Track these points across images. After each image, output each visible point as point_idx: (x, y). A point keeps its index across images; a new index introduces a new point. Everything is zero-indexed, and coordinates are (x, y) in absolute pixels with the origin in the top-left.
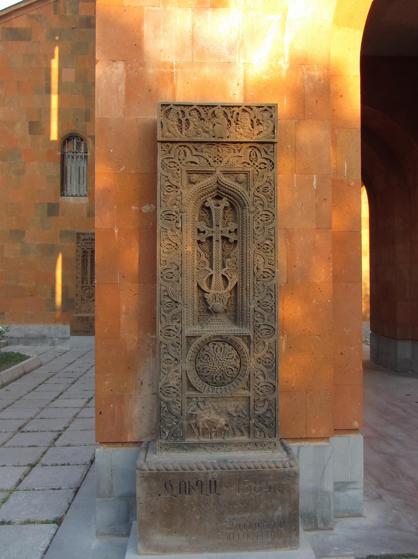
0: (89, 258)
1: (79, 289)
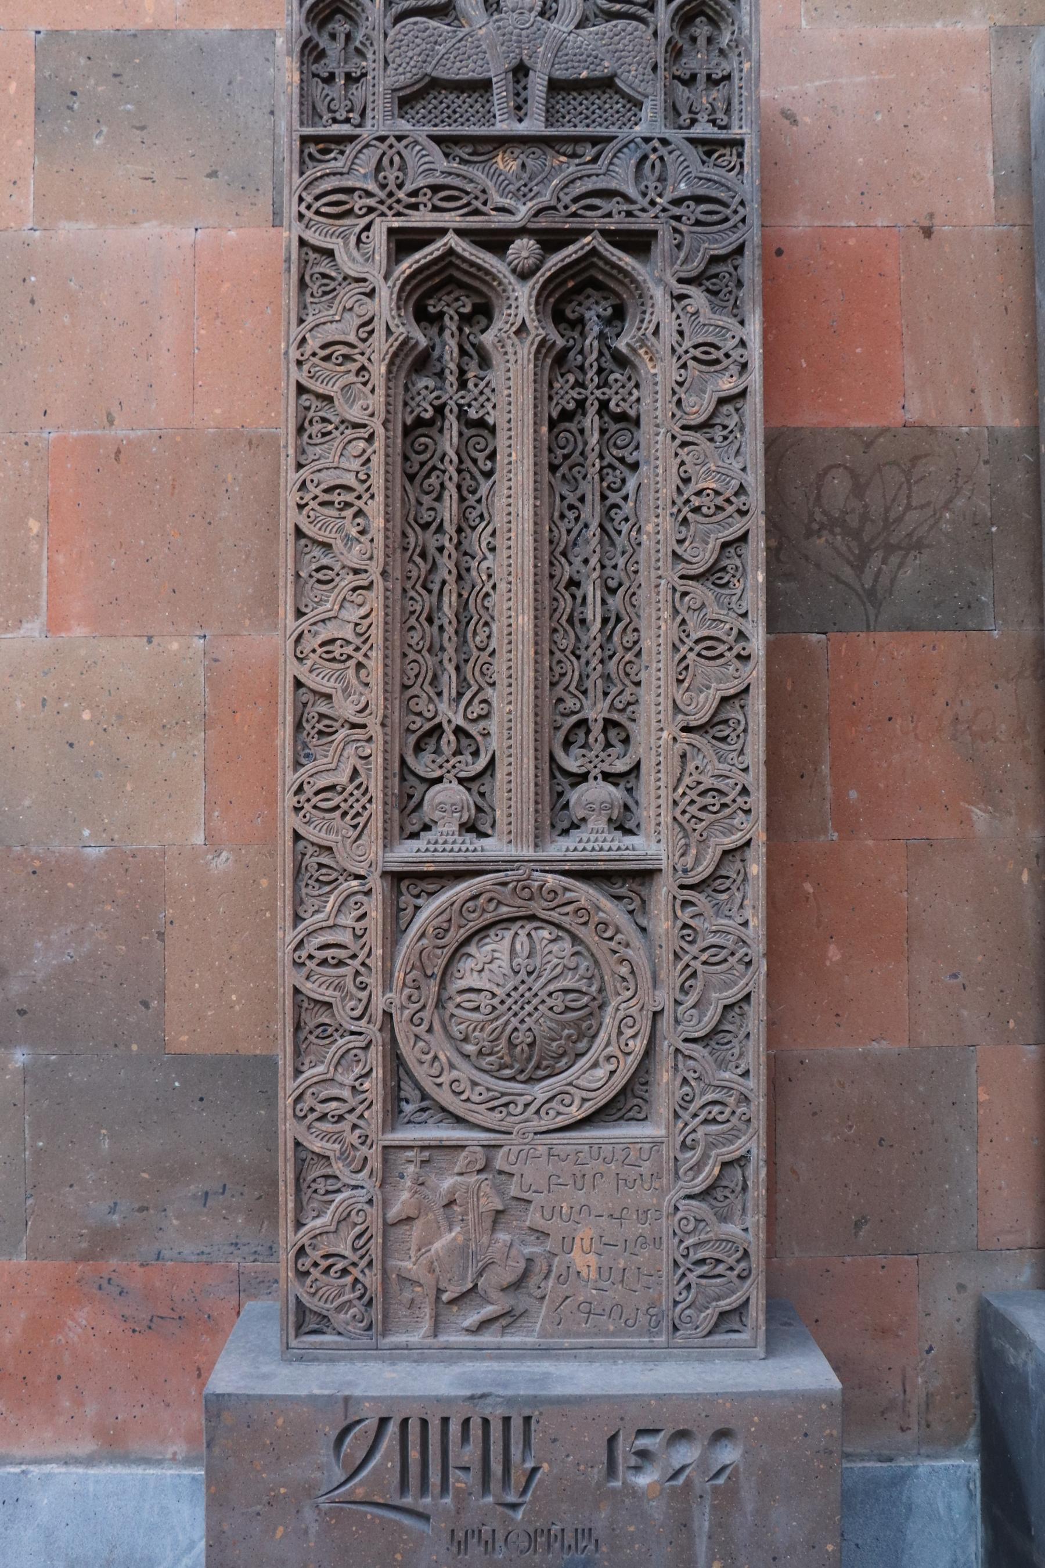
1: (348, 916)
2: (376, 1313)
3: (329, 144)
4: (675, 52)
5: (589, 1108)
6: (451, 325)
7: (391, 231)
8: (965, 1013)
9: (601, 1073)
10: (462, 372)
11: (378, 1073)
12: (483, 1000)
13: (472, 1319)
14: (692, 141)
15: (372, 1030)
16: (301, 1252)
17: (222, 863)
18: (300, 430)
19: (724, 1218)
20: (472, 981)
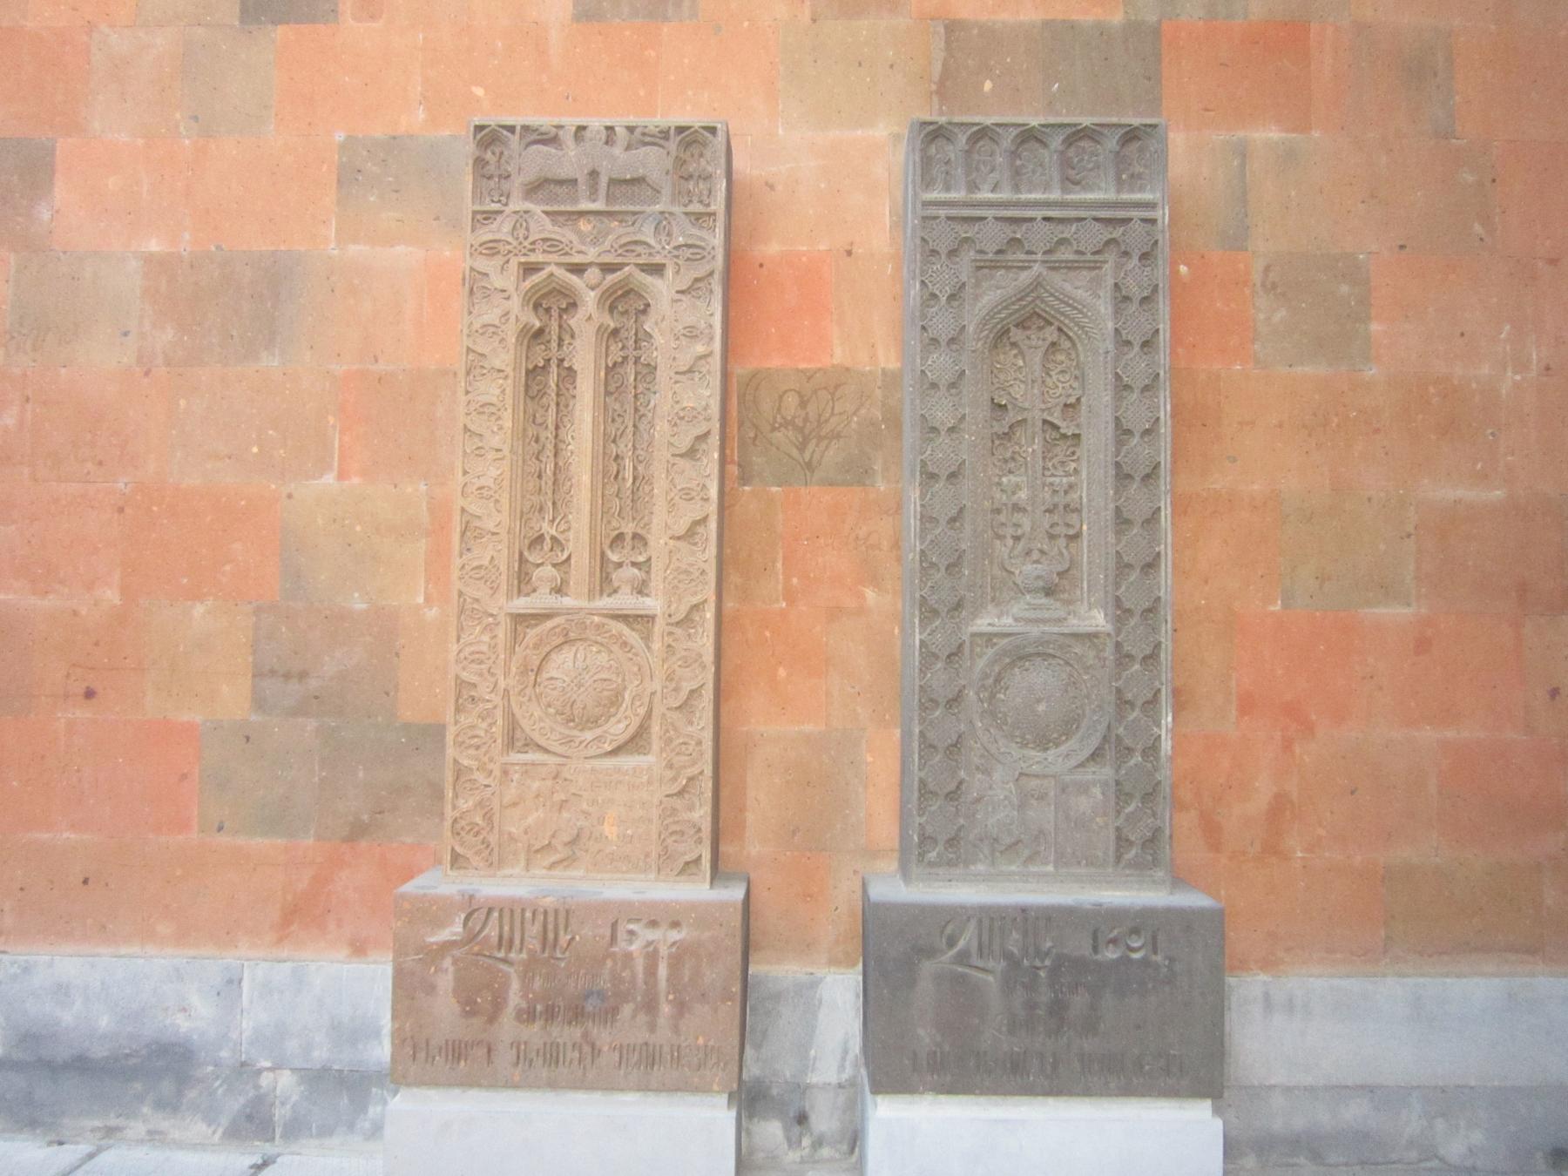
0: (585, 357)
2: (495, 858)
3: (489, 216)
4: (680, 162)
5: (615, 745)
6: (555, 313)
7: (520, 264)
8: (859, 710)
9: (622, 726)
10: (561, 340)
11: (500, 722)
12: (559, 684)
13: (546, 863)
14: (686, 214)
15: (497, 699)
16: (455, 821)
17: (432, 613)
18: (468, 373)
19: (691, 808)
20: (554, 674)
